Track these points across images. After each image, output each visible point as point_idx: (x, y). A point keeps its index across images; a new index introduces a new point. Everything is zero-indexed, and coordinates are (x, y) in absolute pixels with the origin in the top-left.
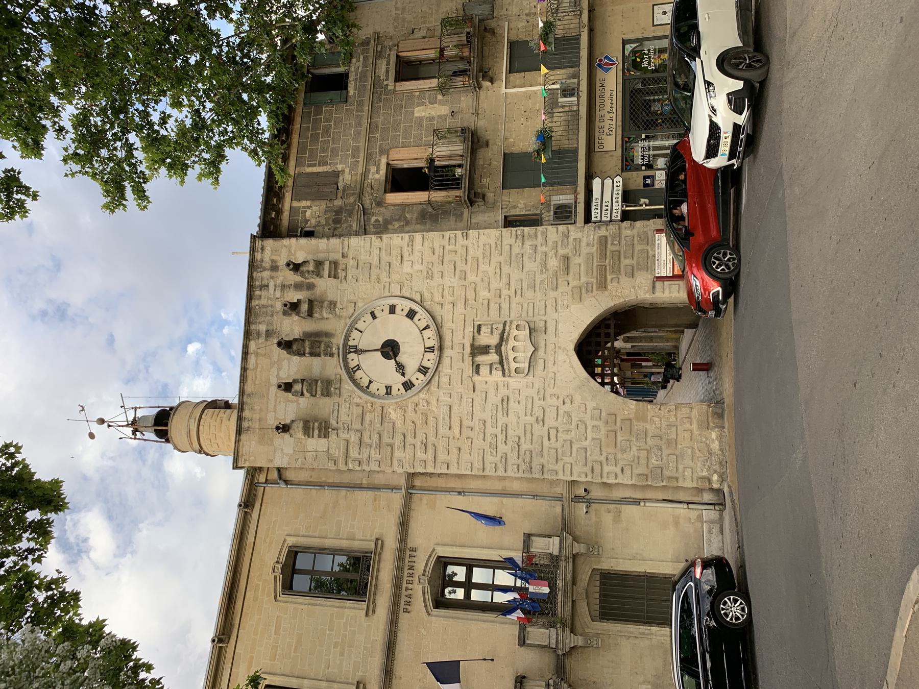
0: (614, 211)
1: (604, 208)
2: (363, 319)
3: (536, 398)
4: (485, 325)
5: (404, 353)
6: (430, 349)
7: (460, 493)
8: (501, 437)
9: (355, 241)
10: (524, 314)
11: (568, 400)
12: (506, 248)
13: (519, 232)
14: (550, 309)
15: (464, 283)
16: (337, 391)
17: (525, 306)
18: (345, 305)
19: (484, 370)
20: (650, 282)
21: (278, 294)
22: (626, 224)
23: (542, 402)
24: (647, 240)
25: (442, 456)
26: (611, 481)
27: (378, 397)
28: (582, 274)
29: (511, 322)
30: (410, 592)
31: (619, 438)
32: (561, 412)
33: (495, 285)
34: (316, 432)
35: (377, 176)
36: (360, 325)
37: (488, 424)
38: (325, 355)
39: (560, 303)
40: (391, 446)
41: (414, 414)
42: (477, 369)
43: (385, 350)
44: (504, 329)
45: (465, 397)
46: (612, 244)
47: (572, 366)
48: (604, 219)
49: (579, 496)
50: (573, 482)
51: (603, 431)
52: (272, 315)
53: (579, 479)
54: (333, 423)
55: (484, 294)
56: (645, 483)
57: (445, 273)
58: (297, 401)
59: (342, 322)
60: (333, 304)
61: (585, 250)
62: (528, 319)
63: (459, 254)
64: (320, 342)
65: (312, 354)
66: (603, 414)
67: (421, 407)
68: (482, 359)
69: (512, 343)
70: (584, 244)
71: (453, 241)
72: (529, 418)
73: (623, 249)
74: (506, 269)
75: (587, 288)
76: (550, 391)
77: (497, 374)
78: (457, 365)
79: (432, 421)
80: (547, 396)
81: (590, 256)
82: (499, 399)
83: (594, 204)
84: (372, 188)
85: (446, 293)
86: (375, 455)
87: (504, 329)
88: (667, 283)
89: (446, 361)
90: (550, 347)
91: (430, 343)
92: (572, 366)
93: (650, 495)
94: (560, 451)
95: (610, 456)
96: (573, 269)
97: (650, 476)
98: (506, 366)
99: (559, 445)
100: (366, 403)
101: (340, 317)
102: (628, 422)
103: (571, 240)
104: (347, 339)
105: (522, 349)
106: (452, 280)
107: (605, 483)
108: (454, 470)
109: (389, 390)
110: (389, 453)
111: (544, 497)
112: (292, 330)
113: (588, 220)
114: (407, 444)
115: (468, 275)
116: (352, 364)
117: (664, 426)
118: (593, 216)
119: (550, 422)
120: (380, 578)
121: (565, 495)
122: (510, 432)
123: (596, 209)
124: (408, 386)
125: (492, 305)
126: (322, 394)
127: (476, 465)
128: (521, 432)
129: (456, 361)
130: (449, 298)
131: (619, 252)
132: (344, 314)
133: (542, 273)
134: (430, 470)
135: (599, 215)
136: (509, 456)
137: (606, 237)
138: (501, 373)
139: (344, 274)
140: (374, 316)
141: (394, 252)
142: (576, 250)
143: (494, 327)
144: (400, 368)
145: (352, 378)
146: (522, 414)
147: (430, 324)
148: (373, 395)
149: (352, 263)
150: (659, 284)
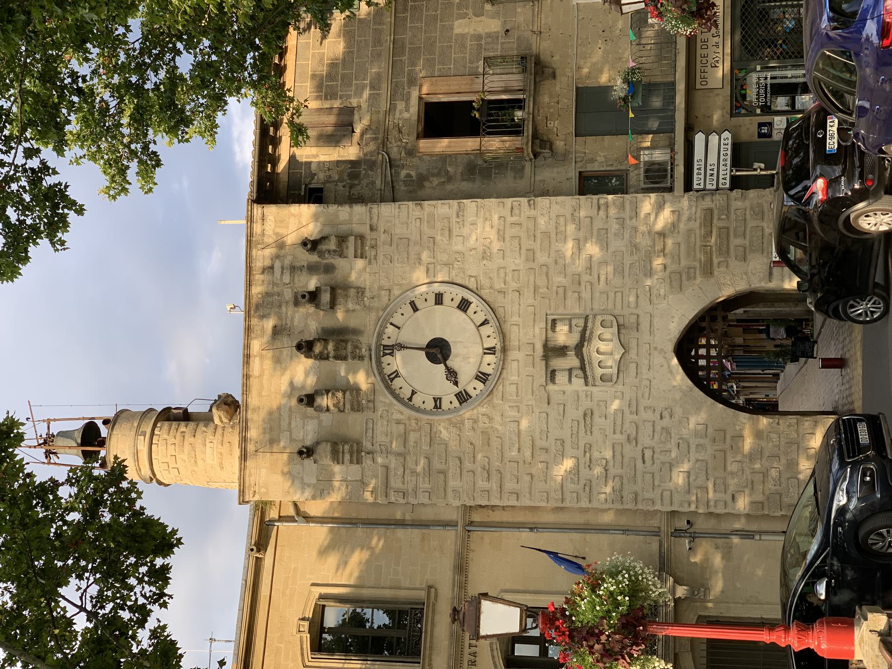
0: (721, 177)
1: (709, 172)
2: (400, 311)
3: (627, 411)
4: (561, 320)
5: (457, 356)
6: (491, 351)
7: (531, 529)
9: (387, 210)
11: (666, 414)
13: (602, 201)
15: (532, 265)
16: (371, 405)
17: (612, 295)
18: (375, 293)
19: (561, 378)
20: (766, 267)
21: (287, 279)
22: (737, 193)
23: (634, 417)
25: (509, 485)
26: (720, 510)
27: (424, 412)
28: (682, 255)
29: (595, 316)
30: (473, 649)
34: (347, 457)
35: (406, 115)
36: (397, 319)
38: (354, 358)
40: (444, 472)
41: (471, 433)
42: (552, 375)
43: (431, 351)
44: (585, 326)
46: (719, 219)
48: (709, 187)
49: (685, 528)
50: (673, 513)
52: (280, 306)
53: (681, 509)
54: (367, 445)
56: (760, 513)
58: (318, 418)
59: (373, 315)
60: (360, 291)
62: (616, 312)
64: (346, 342)
65: (337, 357)
66: (710, 430)
67: (481, 424)
68: (558, 363)
71: (516, 211)
72: (618, 436)
73: (732, 226)
75: (688, 273)
76: (644, 402)
77: (578, 382)
79: (495, 442)
80: (641, 409)
83: (696, 167)
84: (400, 132)
86: (424, 485)
87: (585, 326)
89: (512, 366)
93: (765, 526)
97: (766, 504)
98: (588, 373)
99: (656, 468)
100: (409, 419)
101: (369, 309)
104: (380, 336)
107: (711, 513)
108: (526, 502)
109: (438, 401)
110: (441, 483)
111: (637, 532)
112: (306, 325)
113: (688, 186)
114: (464, 472)
115: (538, 254)
116: (388, 370)
117: (782, 443)
118: (695, 182)
119: (645, 440)
120: (435, 634)
121: (664, 528)
123: (699, 174)
124: (463, 398)
125: (569, 294)
126: (353, 409)
127: (552, 494)
129: (523, 368)
131: (728, 228)
132: (375, 304)
133: (632, 254)
134: (495, 502)
135: (702, 181)
136: (594, 484)
138: (582, 381)
139: (373, 253)
140: (415, 309)
141: (438, 225)
143: (574, 322)
144: (452, 375)
145: (388, 388)
146: (609, 431)
147: (489, 318)
148: (418, 410)
149: (383, 237)
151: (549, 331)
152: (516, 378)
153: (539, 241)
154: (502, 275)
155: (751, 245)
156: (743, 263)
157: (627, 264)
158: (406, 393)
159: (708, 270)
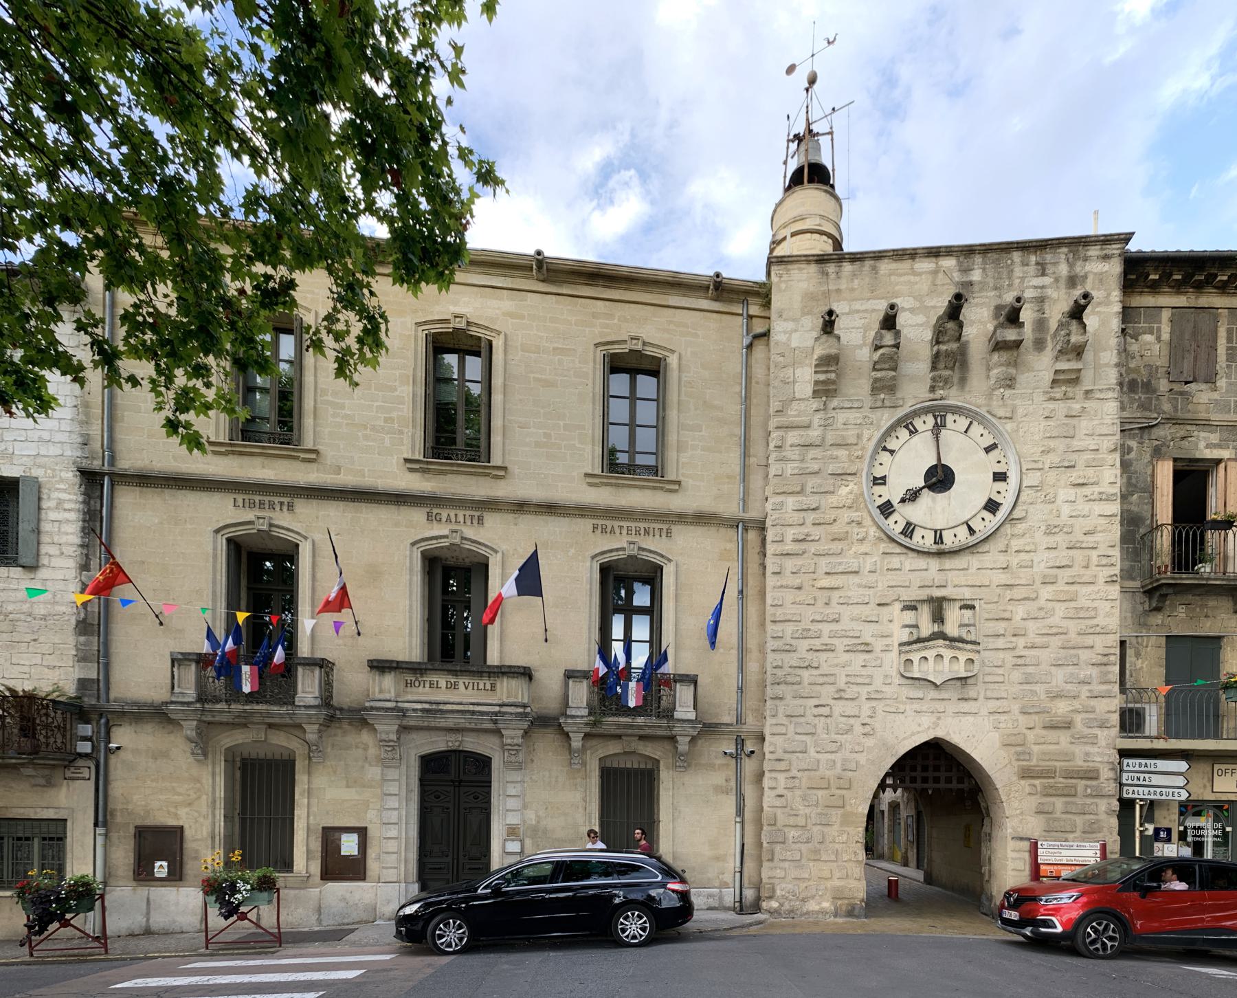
0: (1136, 789)
1: (1142, 776)
3: (870, 688)
4: (974, 615)
8: (817, 643)
10: (988, 670)
11: (867, 729)
12: (1089, 640)
13: (1112, 658)
14: (993, 705)
15: (1038, 582)
17: (1000, 671)
19: (909, 617)
20: (1029, 835)
23: (864, 696)
24: (1089, 832)
29: (978, 652)
31: (820, 793)
32: (852, 721)
33: (1031, 625)
37: (834, 626)
39: (1002, 718)
42: (911, 607)
45: (871, 592)
46: (1087, 786)
47: (913, 734)
48: (1125, 775)
50: (761, 738)
51: (828, 773)
53: (767, 743)
55: (1020, 611)
57: (1053, 554)
61: (1079, 750)
63: (1082, 571)
69: (948, 654)
70: (1089, 748)
74: (1056, 642)
75: (1024, 753)
76: (880, 706)
77: (905, 636)
78: (916, 580)
80: (874, 703)
81: (1068, 757)
82: (869, 640)
85: (1023, 556)
87: (967, 642)
88: (1027, 856)
89: (921, 562)
90: (940, 706)
91: (948, 538)
92: (913, 734)
94: (802, 720)
95: (797, 781)
96: (1052, 735)
98: (915, 646)
102: (841, 803)
103: (1098, 732)
105: (940, 668)
106: (1043, 565)
115: (1050, 588)
118: (1131, 761)
119: (839, 708)
122: (823, 656)
125: (1003, 624)
128: (825, 669)
130: (1015, 560)
133: (1048, 692)
137: (1096, 778)
138: (905, 639)
142: (1079, 739)
143: (972, 629)
146: (849, 670)
150: (1026, 845)
151: (961, 603)
152: (908, 568)
153: (1067, 588)
154: (1027, 548)
155: (1055, 820)
156: (1034, 810)
157: (1037, 688)
159: (1026, 774)
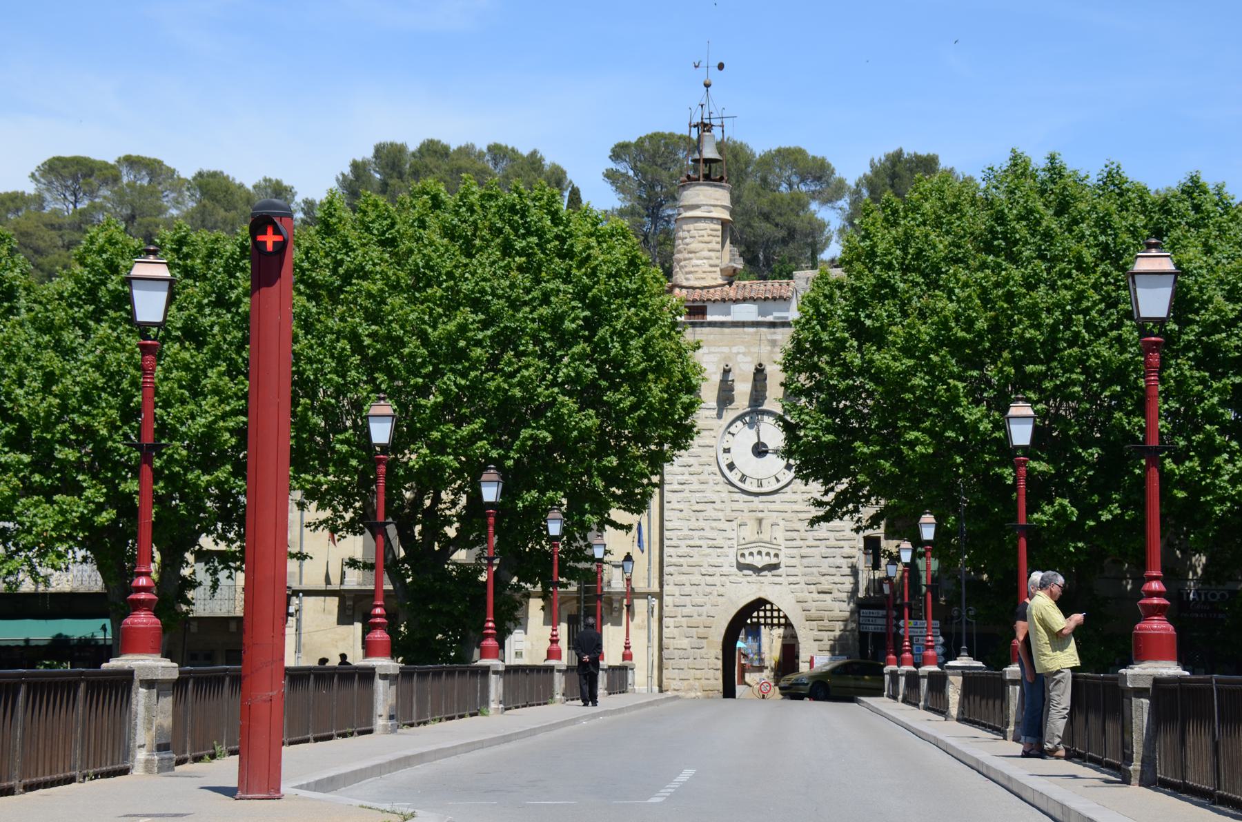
37: (701, 533)
79: (703, 487)
80: (724, 578)
158: (732, 429)
